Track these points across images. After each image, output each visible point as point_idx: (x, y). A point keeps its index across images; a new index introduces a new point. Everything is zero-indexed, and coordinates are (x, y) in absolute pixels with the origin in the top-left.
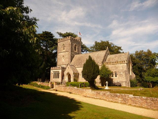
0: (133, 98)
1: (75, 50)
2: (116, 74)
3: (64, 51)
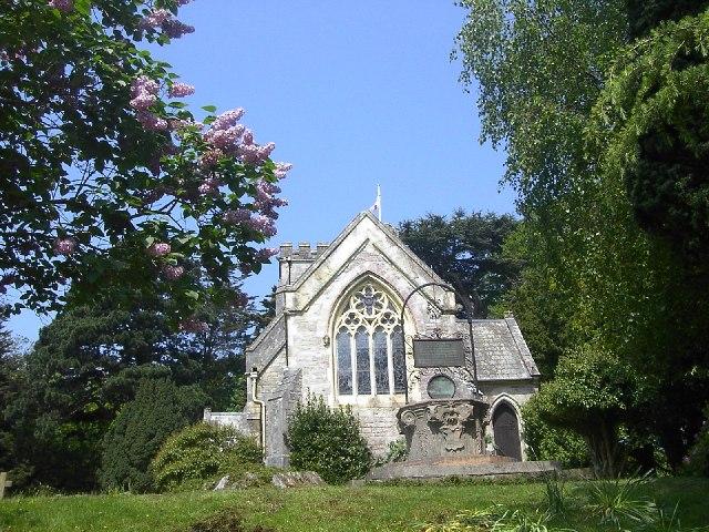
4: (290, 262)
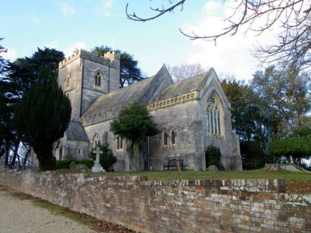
2: (173, 133)
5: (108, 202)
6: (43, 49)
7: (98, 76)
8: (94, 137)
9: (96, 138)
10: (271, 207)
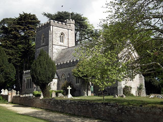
0: (69, 104)
1: (62, 41)
3: (43, 44)
4: (52, 26)
5: (79, 109)
6: (22, 14)
7: (62, 36)
8: (62, 76)
9: (63, 77)
10: (116, 109)
